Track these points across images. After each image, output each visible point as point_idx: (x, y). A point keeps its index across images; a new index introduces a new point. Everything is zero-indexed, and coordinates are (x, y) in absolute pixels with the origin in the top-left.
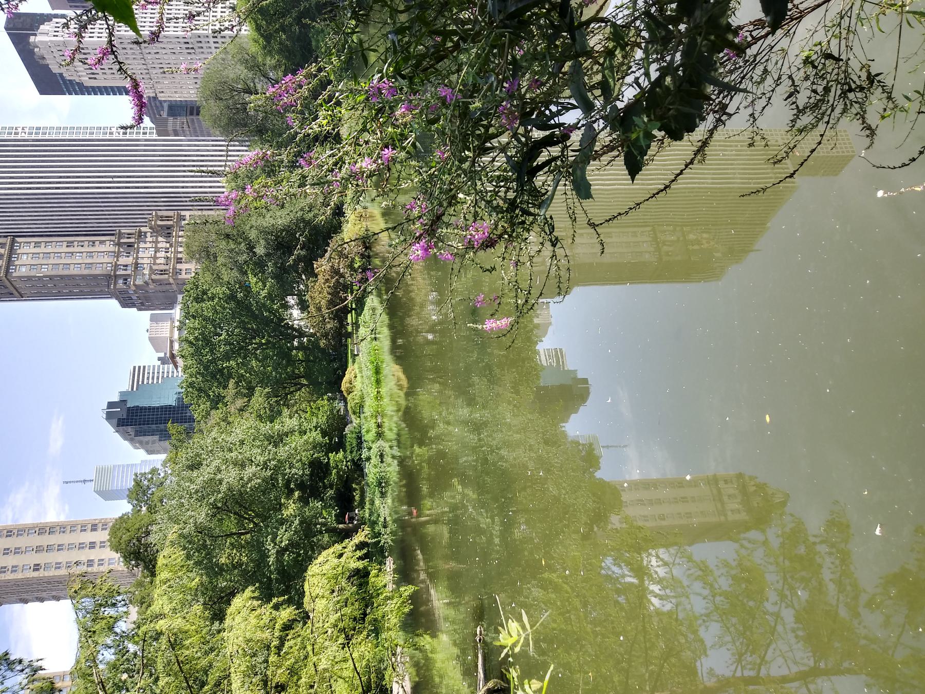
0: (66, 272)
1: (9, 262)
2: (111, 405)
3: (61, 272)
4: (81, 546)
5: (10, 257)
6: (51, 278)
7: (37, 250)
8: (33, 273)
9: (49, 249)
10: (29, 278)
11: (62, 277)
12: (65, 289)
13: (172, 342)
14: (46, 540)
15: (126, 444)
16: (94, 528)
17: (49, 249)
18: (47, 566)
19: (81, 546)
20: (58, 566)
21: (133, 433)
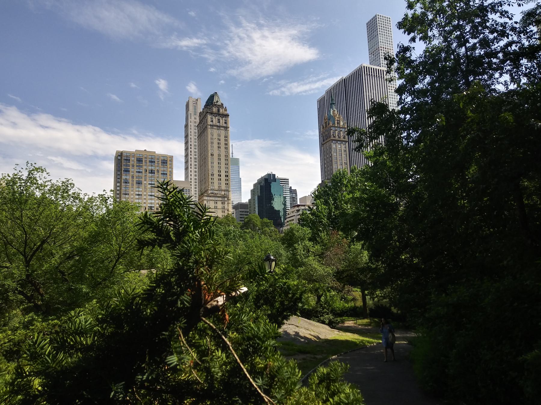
0: (334, 163)
2: (274, 175)
4: (219, 171)
6: (331, 157)
7: (343, 151)
8: (333, 150)
9: (343, 156)
10: (331, 148)
11: (332, 161)
12: (327, 161)
14: (223, 158)
15: (256, 182)
16: (227, 176)
17: (343, 156)
18: (212, 159)
19: (219, 171)
20: (212, 163)
21: (262, 185)
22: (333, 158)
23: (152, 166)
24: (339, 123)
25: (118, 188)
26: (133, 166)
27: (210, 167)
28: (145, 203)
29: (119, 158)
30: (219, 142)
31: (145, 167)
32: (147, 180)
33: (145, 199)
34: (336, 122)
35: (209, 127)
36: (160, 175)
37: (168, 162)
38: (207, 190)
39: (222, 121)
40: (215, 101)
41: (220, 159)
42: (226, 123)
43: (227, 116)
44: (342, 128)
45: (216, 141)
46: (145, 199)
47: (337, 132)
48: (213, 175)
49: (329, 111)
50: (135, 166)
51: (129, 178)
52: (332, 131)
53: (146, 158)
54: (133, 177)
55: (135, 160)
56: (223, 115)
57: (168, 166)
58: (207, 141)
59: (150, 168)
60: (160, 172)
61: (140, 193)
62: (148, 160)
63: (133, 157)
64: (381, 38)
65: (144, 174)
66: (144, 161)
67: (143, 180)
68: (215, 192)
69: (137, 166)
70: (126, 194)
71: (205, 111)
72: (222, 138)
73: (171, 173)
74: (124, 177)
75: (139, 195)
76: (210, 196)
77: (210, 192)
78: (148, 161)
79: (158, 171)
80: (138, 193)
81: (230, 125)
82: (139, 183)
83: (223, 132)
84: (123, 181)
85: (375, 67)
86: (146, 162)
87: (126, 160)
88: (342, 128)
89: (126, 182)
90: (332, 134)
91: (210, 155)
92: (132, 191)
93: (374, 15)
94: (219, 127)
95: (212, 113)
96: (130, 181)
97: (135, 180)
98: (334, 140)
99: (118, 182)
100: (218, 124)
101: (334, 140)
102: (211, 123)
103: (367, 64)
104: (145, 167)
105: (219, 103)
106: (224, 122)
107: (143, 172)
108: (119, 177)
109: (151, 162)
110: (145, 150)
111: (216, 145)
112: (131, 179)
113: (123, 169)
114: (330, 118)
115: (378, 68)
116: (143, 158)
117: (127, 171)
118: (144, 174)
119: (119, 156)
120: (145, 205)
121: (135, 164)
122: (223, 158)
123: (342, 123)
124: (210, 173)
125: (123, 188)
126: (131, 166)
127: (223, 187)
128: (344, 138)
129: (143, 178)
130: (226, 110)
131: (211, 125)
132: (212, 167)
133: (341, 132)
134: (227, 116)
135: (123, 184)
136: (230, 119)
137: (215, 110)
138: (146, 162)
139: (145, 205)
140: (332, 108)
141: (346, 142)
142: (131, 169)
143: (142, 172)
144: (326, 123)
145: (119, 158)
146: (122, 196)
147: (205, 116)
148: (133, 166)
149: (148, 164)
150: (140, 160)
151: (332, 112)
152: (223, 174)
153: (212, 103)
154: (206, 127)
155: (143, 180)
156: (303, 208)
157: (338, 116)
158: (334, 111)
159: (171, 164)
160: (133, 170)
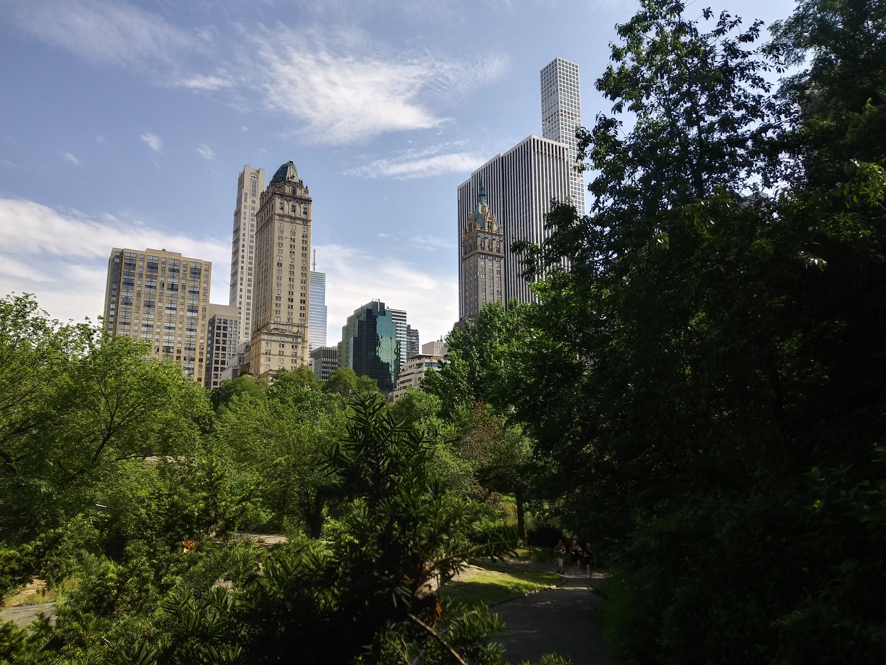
0: (480, 290)
1: (487, 255)
2: (383, 305)
3: (480, 288)
5: (491, 255)
6: (477, 280)
7: (495, 272)
8: (480, 269)
9: (496, 279)
10: (476, 267)
11: (477, 287)
13: (430, 357)
14: (298, 271)
15: (352, 313)
18: (280, 271)
21: (362, 319)
22: (480, 283)
23: (173, 277)
24: (490, 227)
25: (112, 313)
26: (141, 275)
27: (274, 285)
28: (157, 340)
29: (117, 260)
30: (293, 243)
31: (160, 279)
32: (164, 301)
33: (158, 333)
34: (487, 224)
35: (277, 217)
36: (187, 295)
37: (203, 273)
38: (268, 323)
39: (300, 209)
40: (288, 175)
41: (292, 273)
42: (305, 213)
43: (308, 201)
44: (496, 235)
45: (287, 243)
46: (158, 333)
47: (487, 241)
48: (278, 298)
49: (477, 207)
50: (144, 276)
51: (132, 295)
52: (479, 239)
53: (163, 263)
54: (139, 295)
55: (145, 266)
56: (301, 199)
57: (203, 279)
58: (272, 240)
59: (171, 280)
60: (188, 289)
61: (150, 323)
62: (168, 267)
63: (142, 260)
64: (562, 97)
65: (158, 291)
66: (160, 268)
67: (157, 300)
68: (282, 327)
69: (148, 276)
70: (125, 324)
71: (271, 190)
72: (299, 238)
73: (207, 291)
74: (123, 294)
75: (147, 326)
76: (273, 334)
77: (272, 326)
78: (167, 270)
79: (184, 287)
80: (146, 322)
81: (313, 216)
82: (149, 305)
83: (299, 228)
84: (121, 300)
85: (551, 142)
86: (163, 270)
87: (129, 264)
88: (496, 235)
89: (127, 302)
90: (479, 243)
91: (275, 264)
92: (137, 318)
93: (553, 59)
94: (294, 219)
95: (282, 196)
96: (134, 302)
97: (143, 299)
98: (483, 254)
99: (113, 303)
100: (292, 214)
101: (483, 254)
102: (281, 212)
103: (538, 136)
104: (160, 279)
105: (296, 180)
106: (302, 210)
107: (158, 287)
108: (114, 293)
109: (173, 270)
110: (164, 250)
111: (286, 249)
112: (135, 298)
113: (122, 281)
114: (478, 218)
115: (555, 143)
116: (159, 263)
117: (129, 284)
118: (158, 291)
119: (117, 257)
120: (157, 344)
121: (144, 273)
122: (298, 271)
123: (495, 228)
124: (275, 295)
125: (120, 314)
126: (137, 276)
127: (296, 319)
128: (498, 251)
129: (157, 297)
130: (307, 192)
131: (279, 215)
132: (279, 285)
133: (494, 242)
134: (308, 201)
135: (120, 306)
136: (313, 208)
137: (288, 190)
138: (163, 270)
139: (157, 344)
140: (480, 201)
141: (501, 257)
142: (137, 282)
143: (155, 287)
144: (470, 225)
145: (117, 260)
146: (118, 326)
147: (271, 199)
148: (141, 275)
149: (168, 273)
150: (153, 267)
151: (480, 208)
152: (297, 298)
153: (284, 178)
154: (272, 218)
155: (157, 300)
156: (427, 361)
157: (489, 216)
158: (484, 207)
159: (208, 277)
160: (140, 283)
